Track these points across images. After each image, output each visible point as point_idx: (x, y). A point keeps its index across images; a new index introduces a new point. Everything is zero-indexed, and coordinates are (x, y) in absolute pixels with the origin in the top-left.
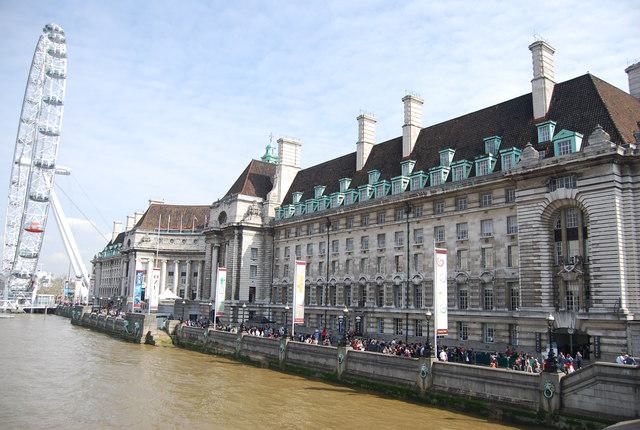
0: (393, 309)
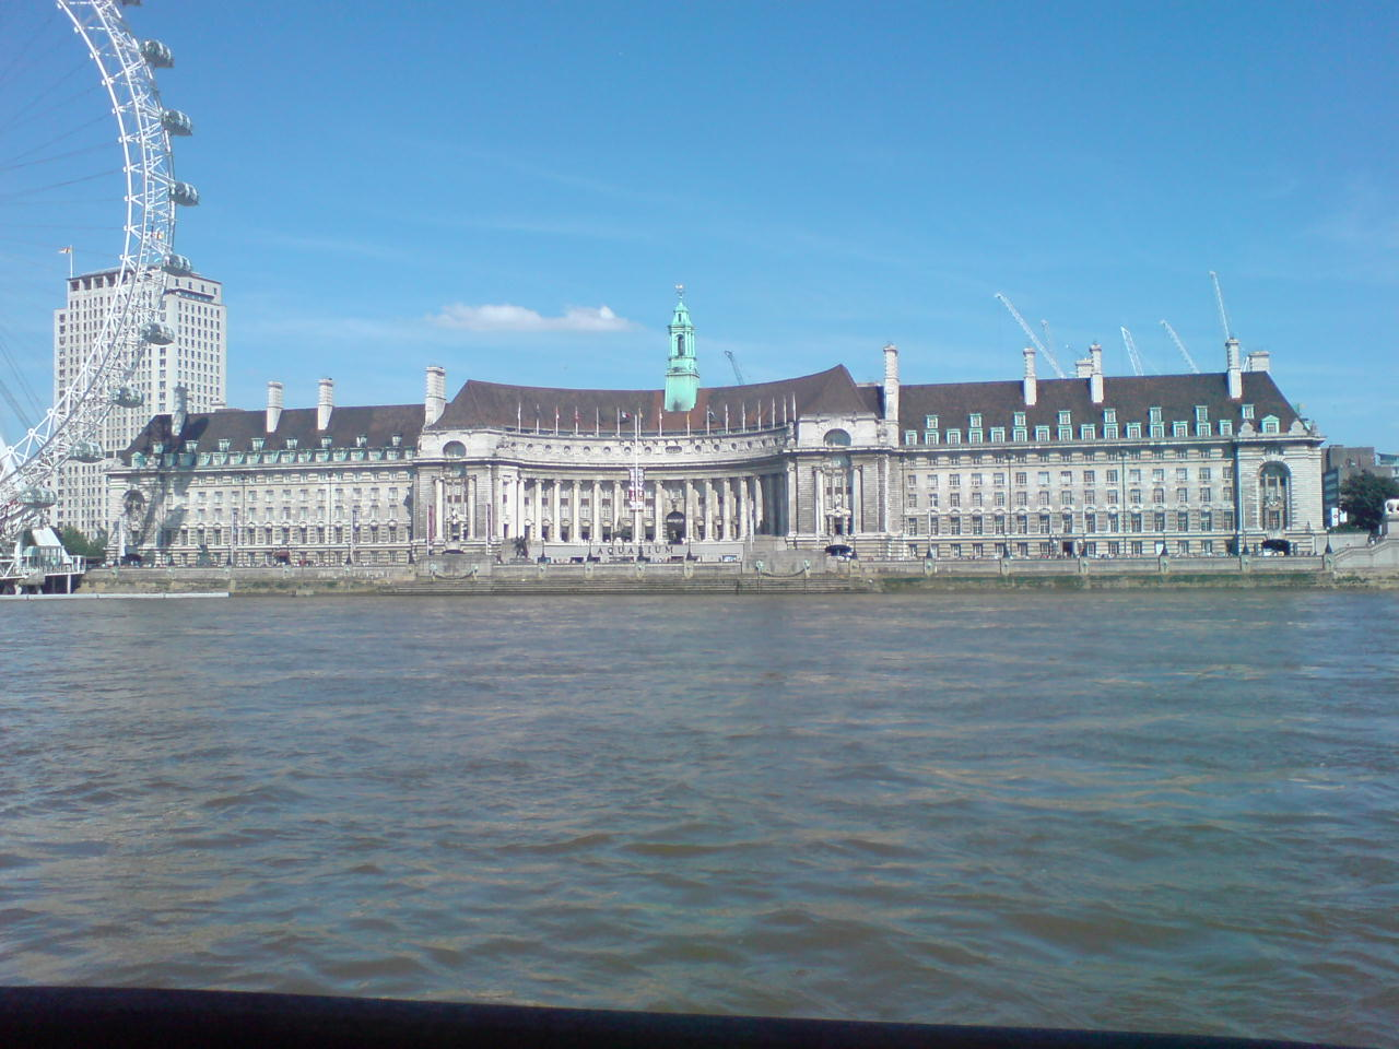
0: (1108, 533)
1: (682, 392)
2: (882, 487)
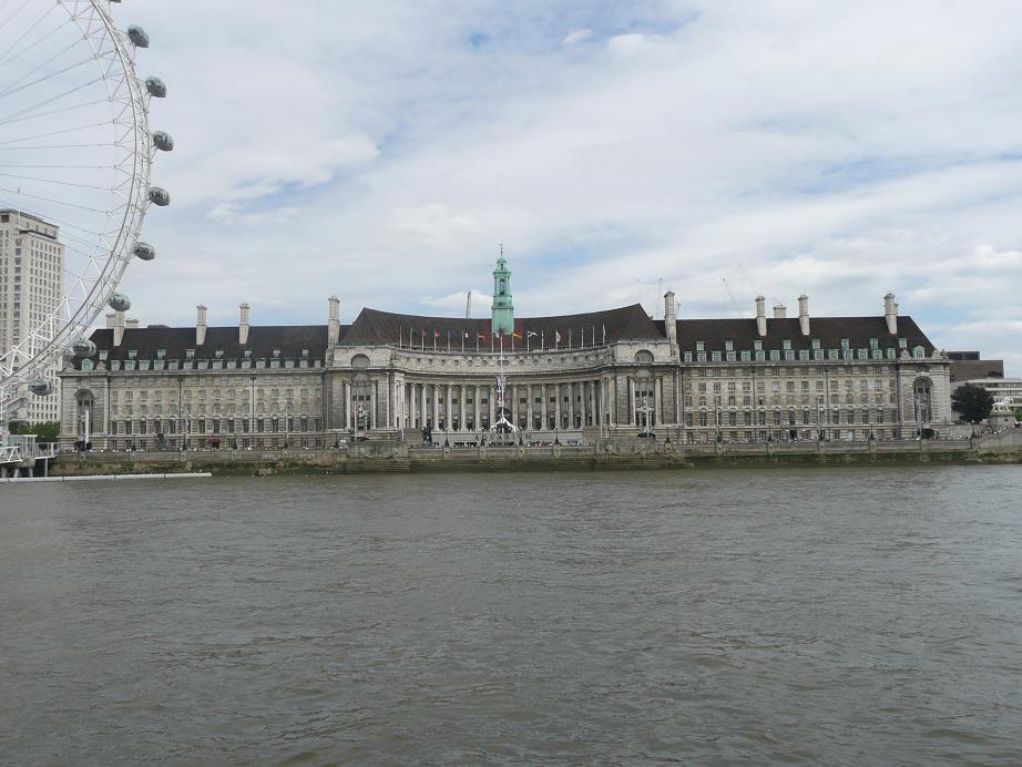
1: (505, 321)
2: (675, 393)
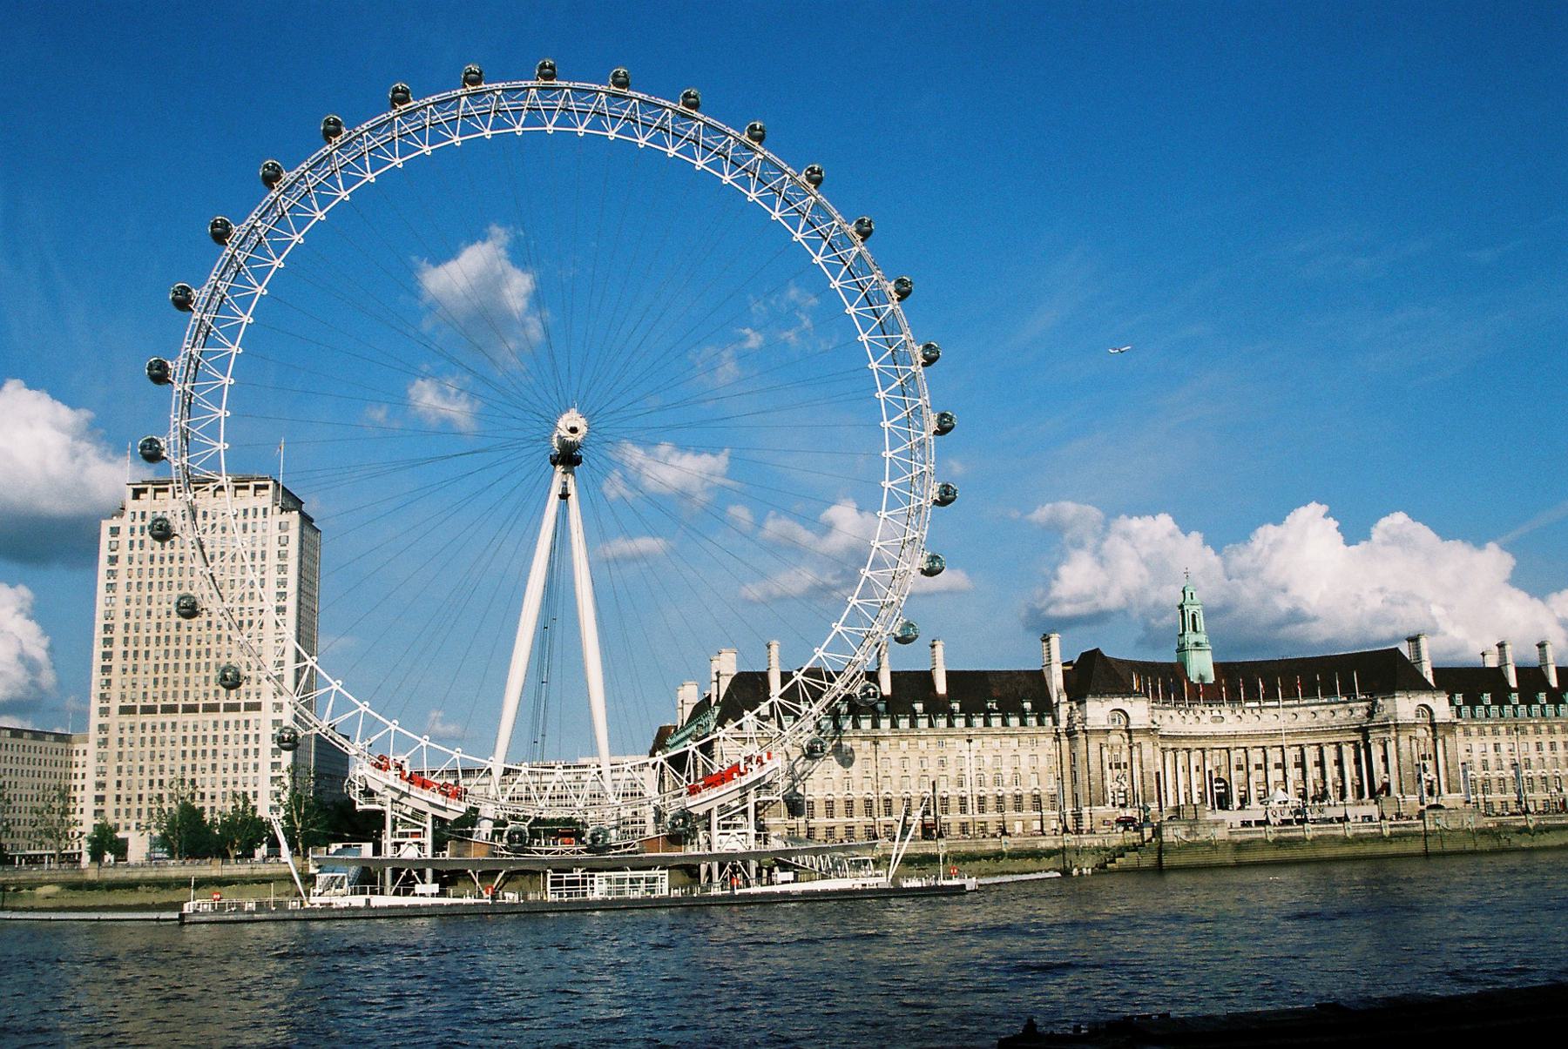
1: (1201, 666)
